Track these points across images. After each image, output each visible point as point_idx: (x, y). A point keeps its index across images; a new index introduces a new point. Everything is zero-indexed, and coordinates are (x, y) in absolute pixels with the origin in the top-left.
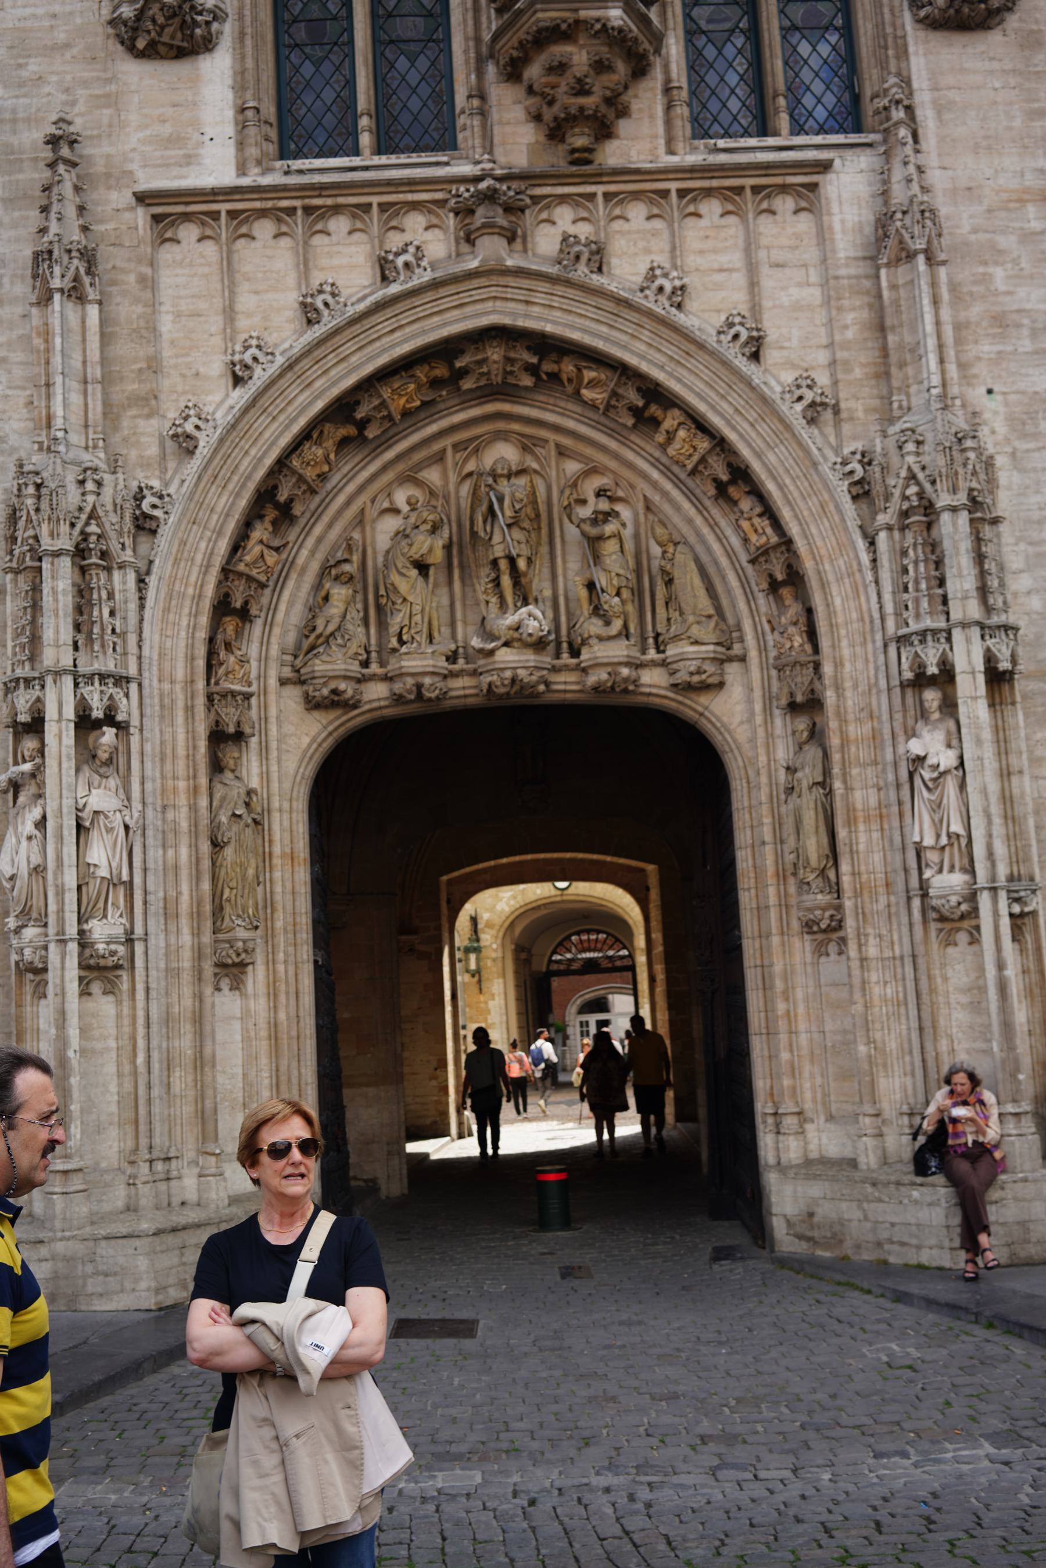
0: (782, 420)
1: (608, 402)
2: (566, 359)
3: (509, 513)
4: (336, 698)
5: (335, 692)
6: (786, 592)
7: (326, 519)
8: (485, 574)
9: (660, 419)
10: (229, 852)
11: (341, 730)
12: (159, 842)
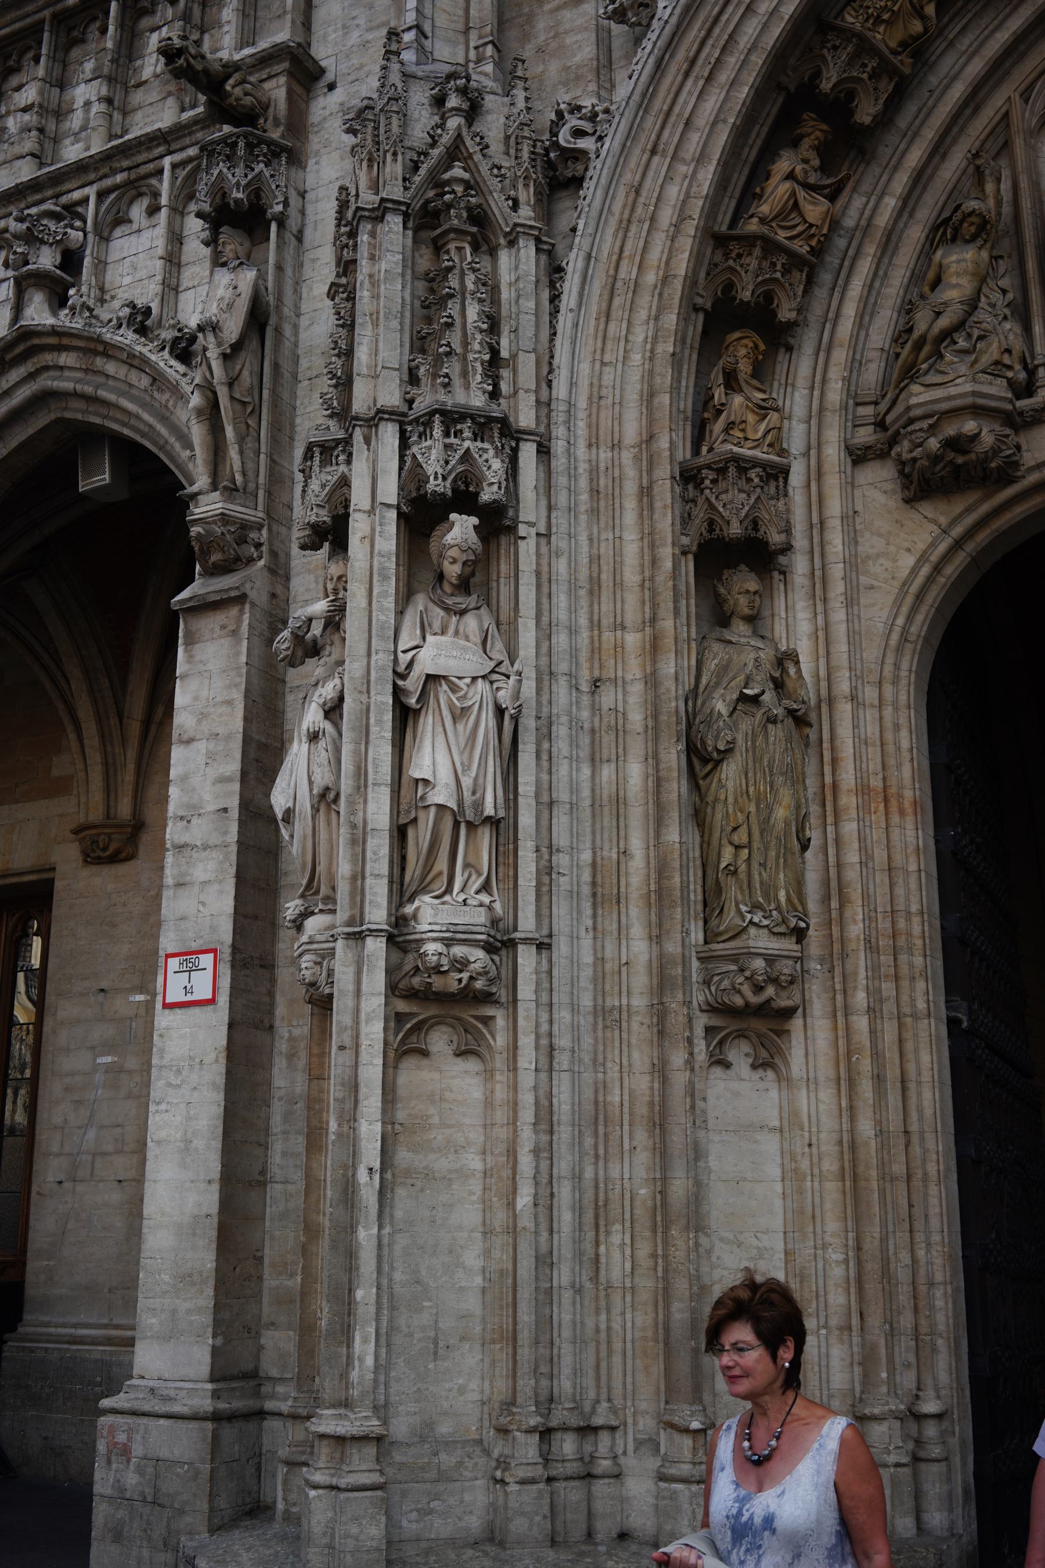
4: (960, 460)
5: (955, 444)
10: (730, 772)
11: (983, 537)
12: (584, 753)
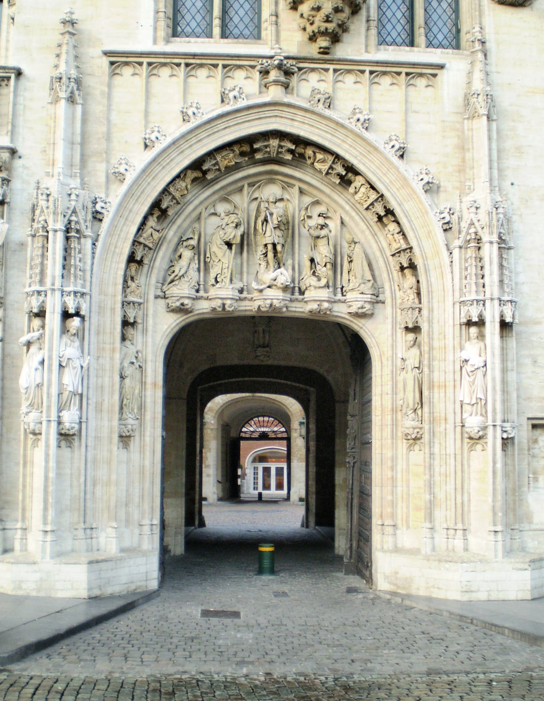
0: (412, 189)
1: (328, 170)
2: (308, 147)
3: (276, 222)
4: (182, 307)
5: (182, 304)
6: (406, 271)
7: (183, 217)
8: (261, 250)
9: (352, 181)
10: (127, 381)
11: (183, 324)
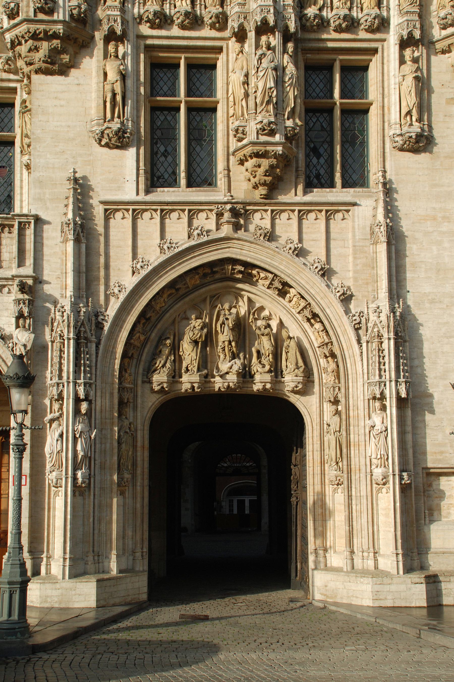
10: (123, 446)
